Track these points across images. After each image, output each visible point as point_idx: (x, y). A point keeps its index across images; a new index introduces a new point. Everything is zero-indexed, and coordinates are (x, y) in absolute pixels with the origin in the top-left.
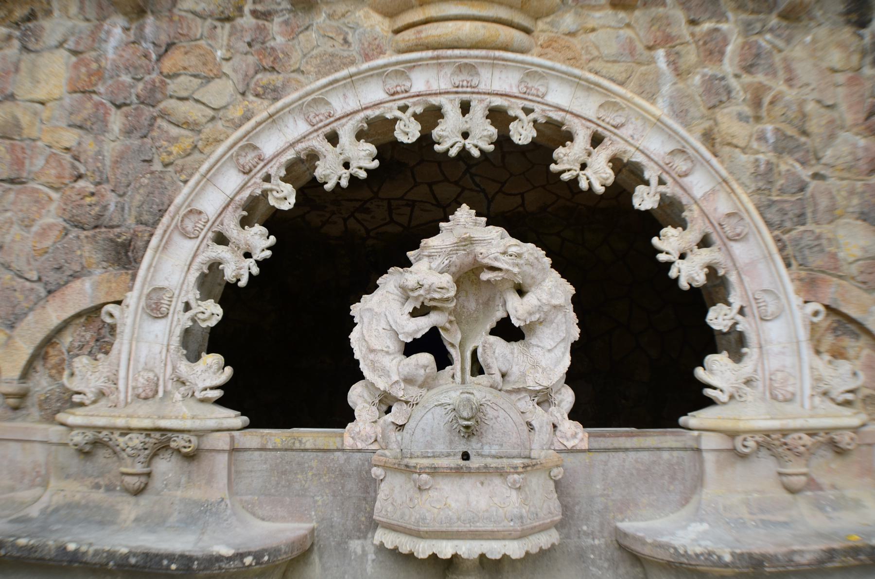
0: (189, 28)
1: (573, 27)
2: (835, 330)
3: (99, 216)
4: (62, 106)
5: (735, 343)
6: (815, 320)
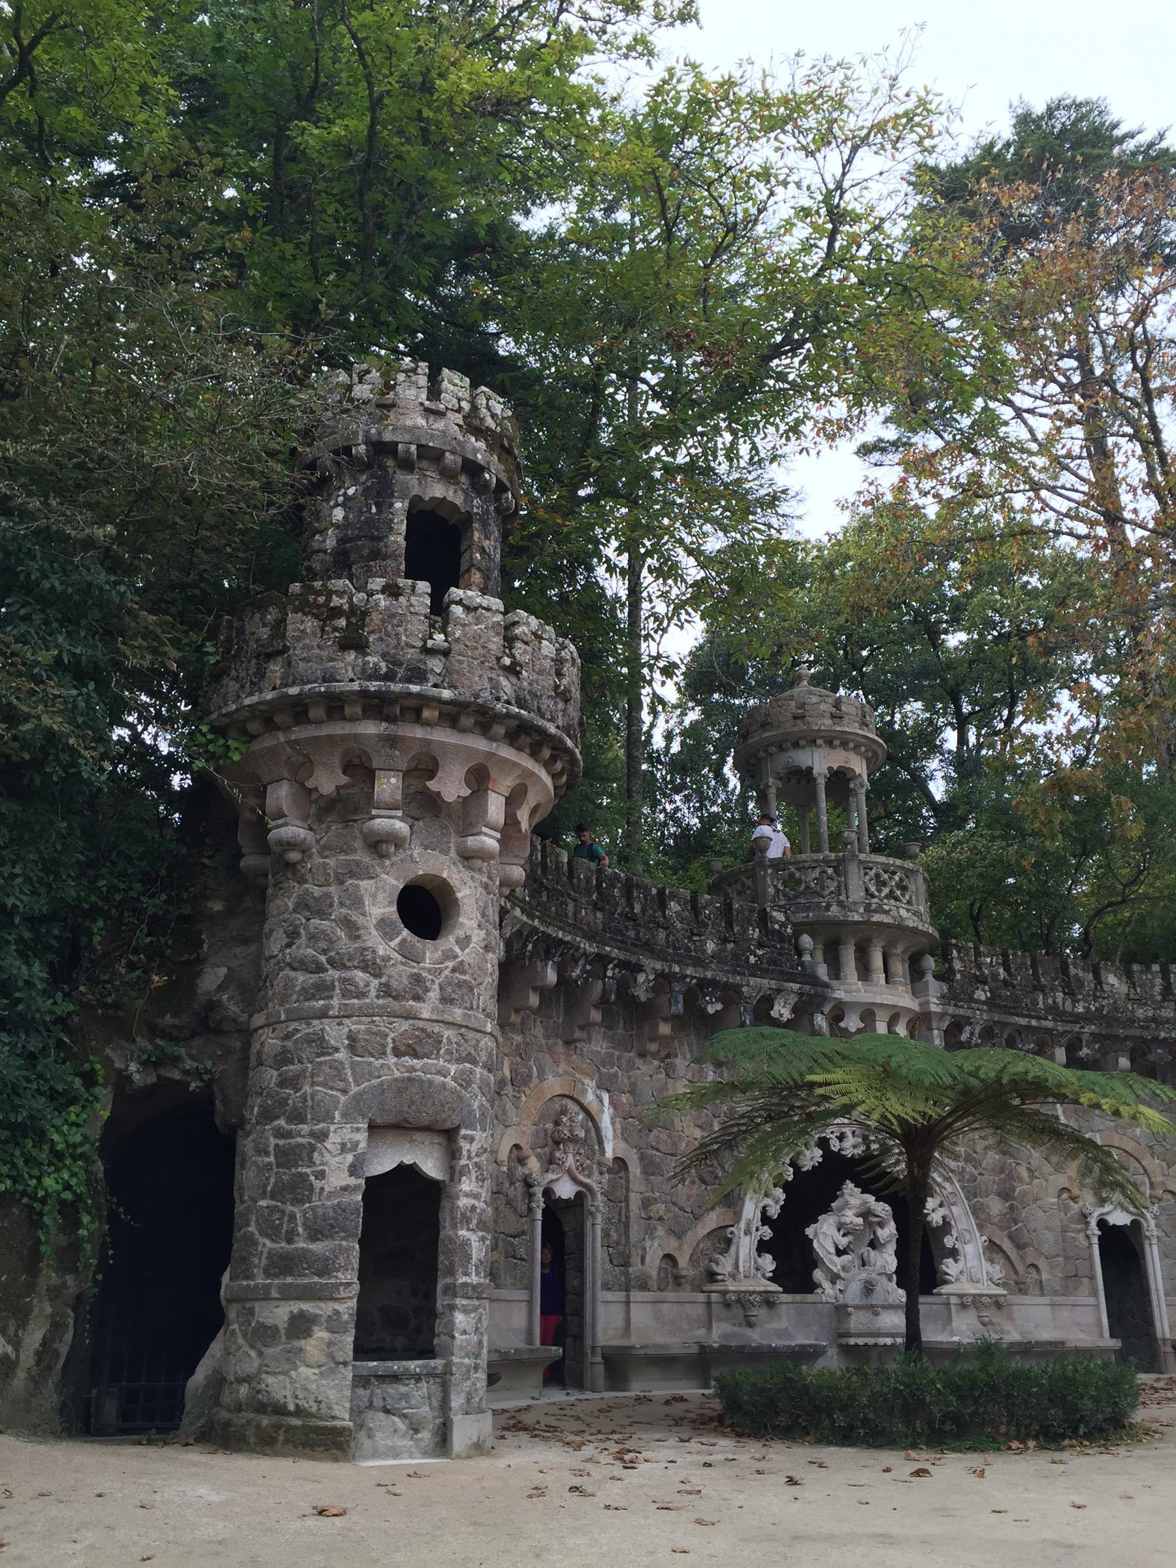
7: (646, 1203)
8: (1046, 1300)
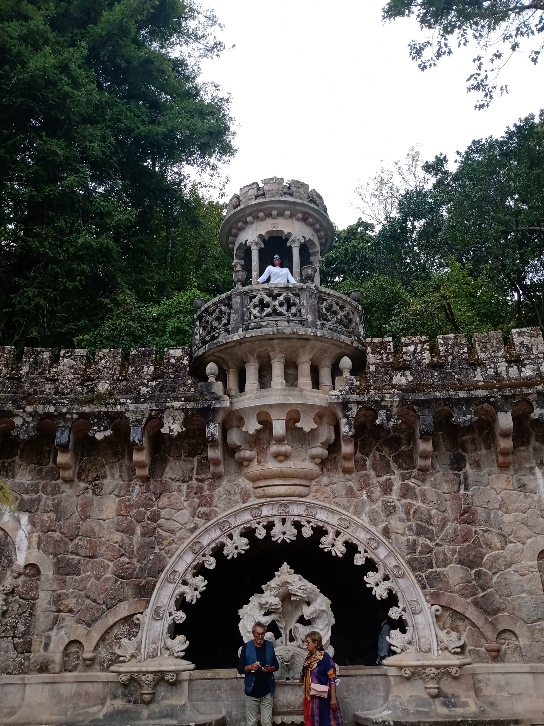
0: (170, 487)
1: (327, 483)
2: (451, 617)
3: (132, 573)
4: (113, 522)
6: (438, 613)
7: (57, 600)
8: (526, 667)
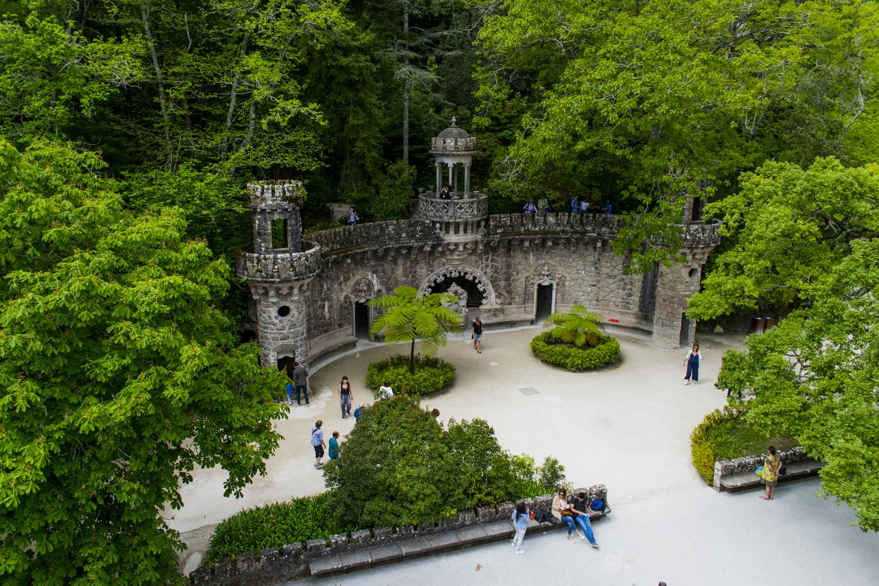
5: (486, 298)
